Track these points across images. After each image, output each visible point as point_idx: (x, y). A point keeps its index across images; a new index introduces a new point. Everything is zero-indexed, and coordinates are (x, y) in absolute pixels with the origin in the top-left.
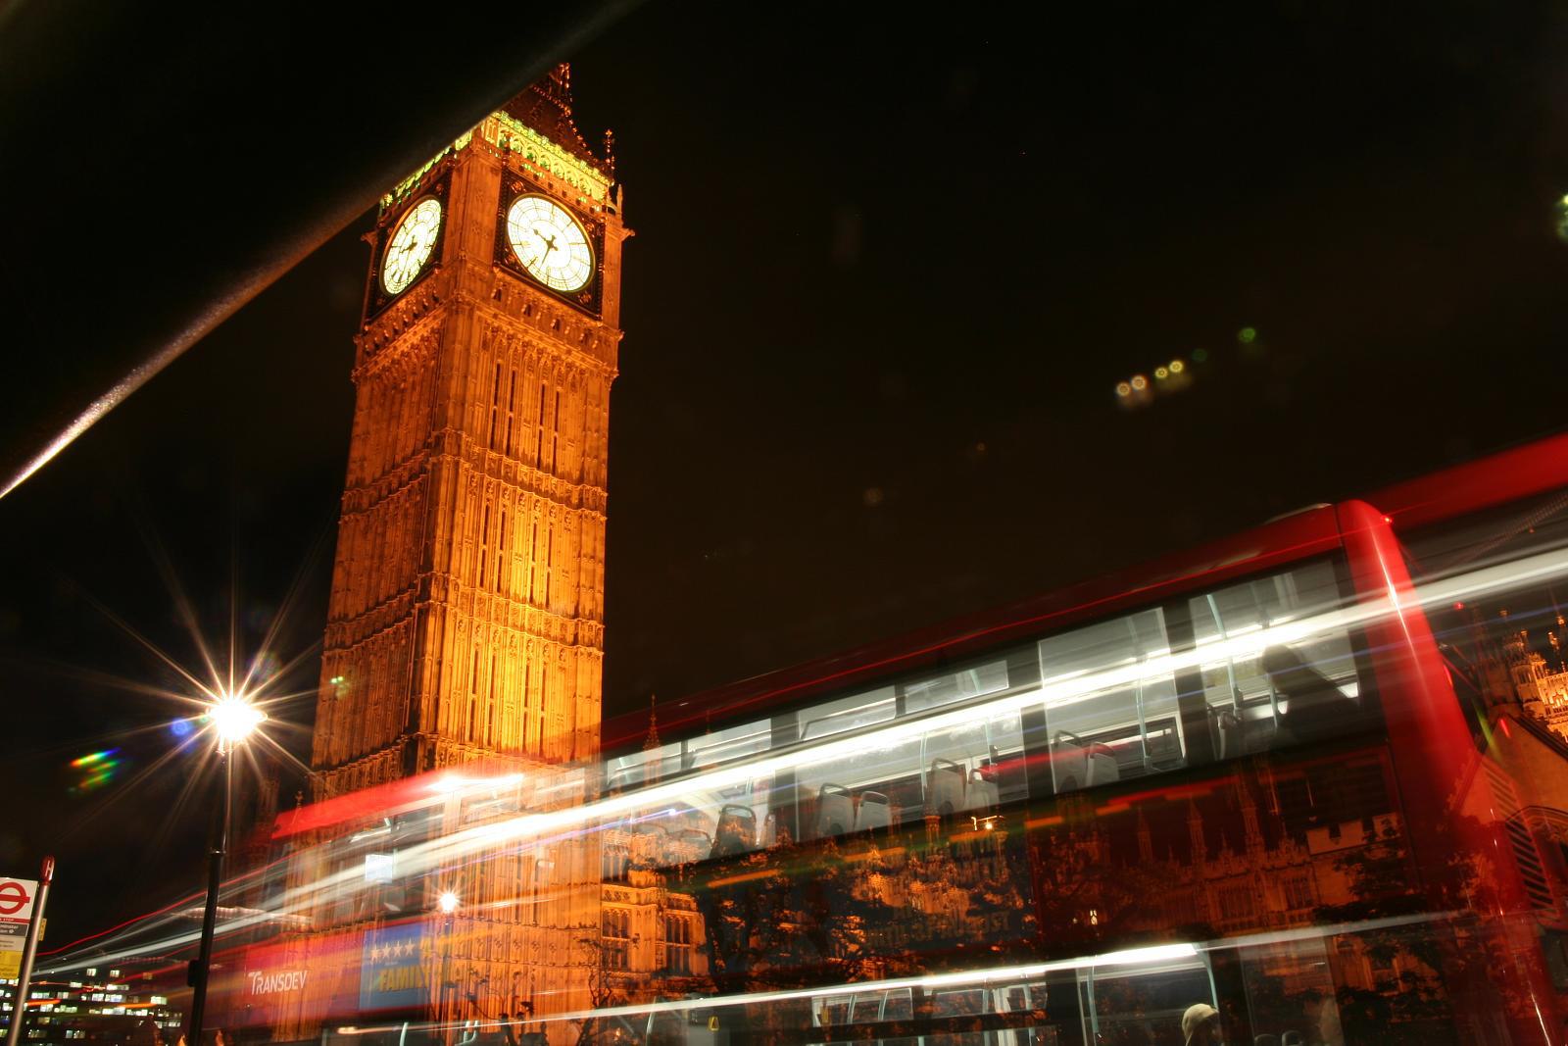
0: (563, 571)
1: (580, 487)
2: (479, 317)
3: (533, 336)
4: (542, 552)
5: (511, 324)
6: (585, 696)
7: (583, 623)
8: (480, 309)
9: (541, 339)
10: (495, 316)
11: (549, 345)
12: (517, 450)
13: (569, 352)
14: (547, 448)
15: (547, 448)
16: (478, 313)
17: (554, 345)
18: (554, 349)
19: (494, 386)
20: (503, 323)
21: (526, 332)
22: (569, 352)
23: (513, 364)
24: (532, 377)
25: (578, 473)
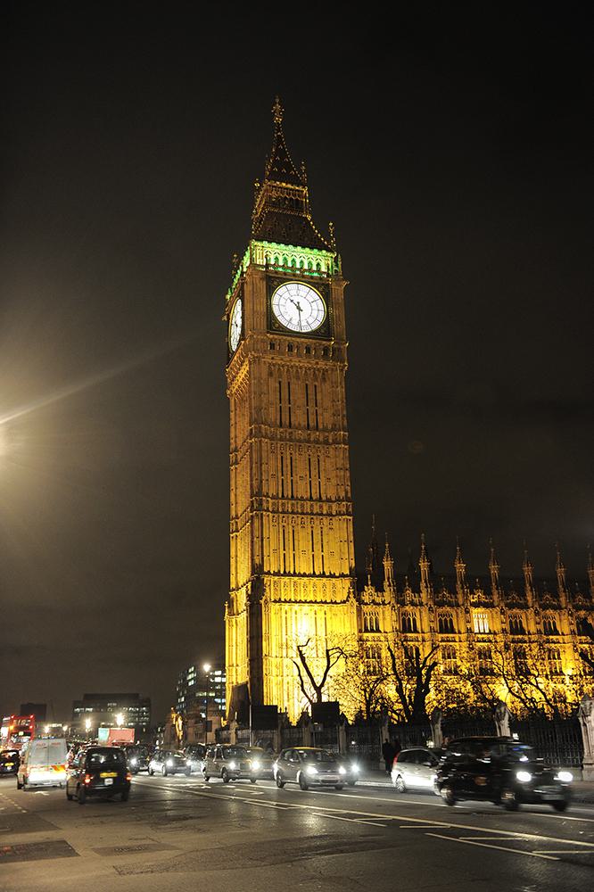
3: (295, 362)
10: (273, 358)
22: (317, 363)
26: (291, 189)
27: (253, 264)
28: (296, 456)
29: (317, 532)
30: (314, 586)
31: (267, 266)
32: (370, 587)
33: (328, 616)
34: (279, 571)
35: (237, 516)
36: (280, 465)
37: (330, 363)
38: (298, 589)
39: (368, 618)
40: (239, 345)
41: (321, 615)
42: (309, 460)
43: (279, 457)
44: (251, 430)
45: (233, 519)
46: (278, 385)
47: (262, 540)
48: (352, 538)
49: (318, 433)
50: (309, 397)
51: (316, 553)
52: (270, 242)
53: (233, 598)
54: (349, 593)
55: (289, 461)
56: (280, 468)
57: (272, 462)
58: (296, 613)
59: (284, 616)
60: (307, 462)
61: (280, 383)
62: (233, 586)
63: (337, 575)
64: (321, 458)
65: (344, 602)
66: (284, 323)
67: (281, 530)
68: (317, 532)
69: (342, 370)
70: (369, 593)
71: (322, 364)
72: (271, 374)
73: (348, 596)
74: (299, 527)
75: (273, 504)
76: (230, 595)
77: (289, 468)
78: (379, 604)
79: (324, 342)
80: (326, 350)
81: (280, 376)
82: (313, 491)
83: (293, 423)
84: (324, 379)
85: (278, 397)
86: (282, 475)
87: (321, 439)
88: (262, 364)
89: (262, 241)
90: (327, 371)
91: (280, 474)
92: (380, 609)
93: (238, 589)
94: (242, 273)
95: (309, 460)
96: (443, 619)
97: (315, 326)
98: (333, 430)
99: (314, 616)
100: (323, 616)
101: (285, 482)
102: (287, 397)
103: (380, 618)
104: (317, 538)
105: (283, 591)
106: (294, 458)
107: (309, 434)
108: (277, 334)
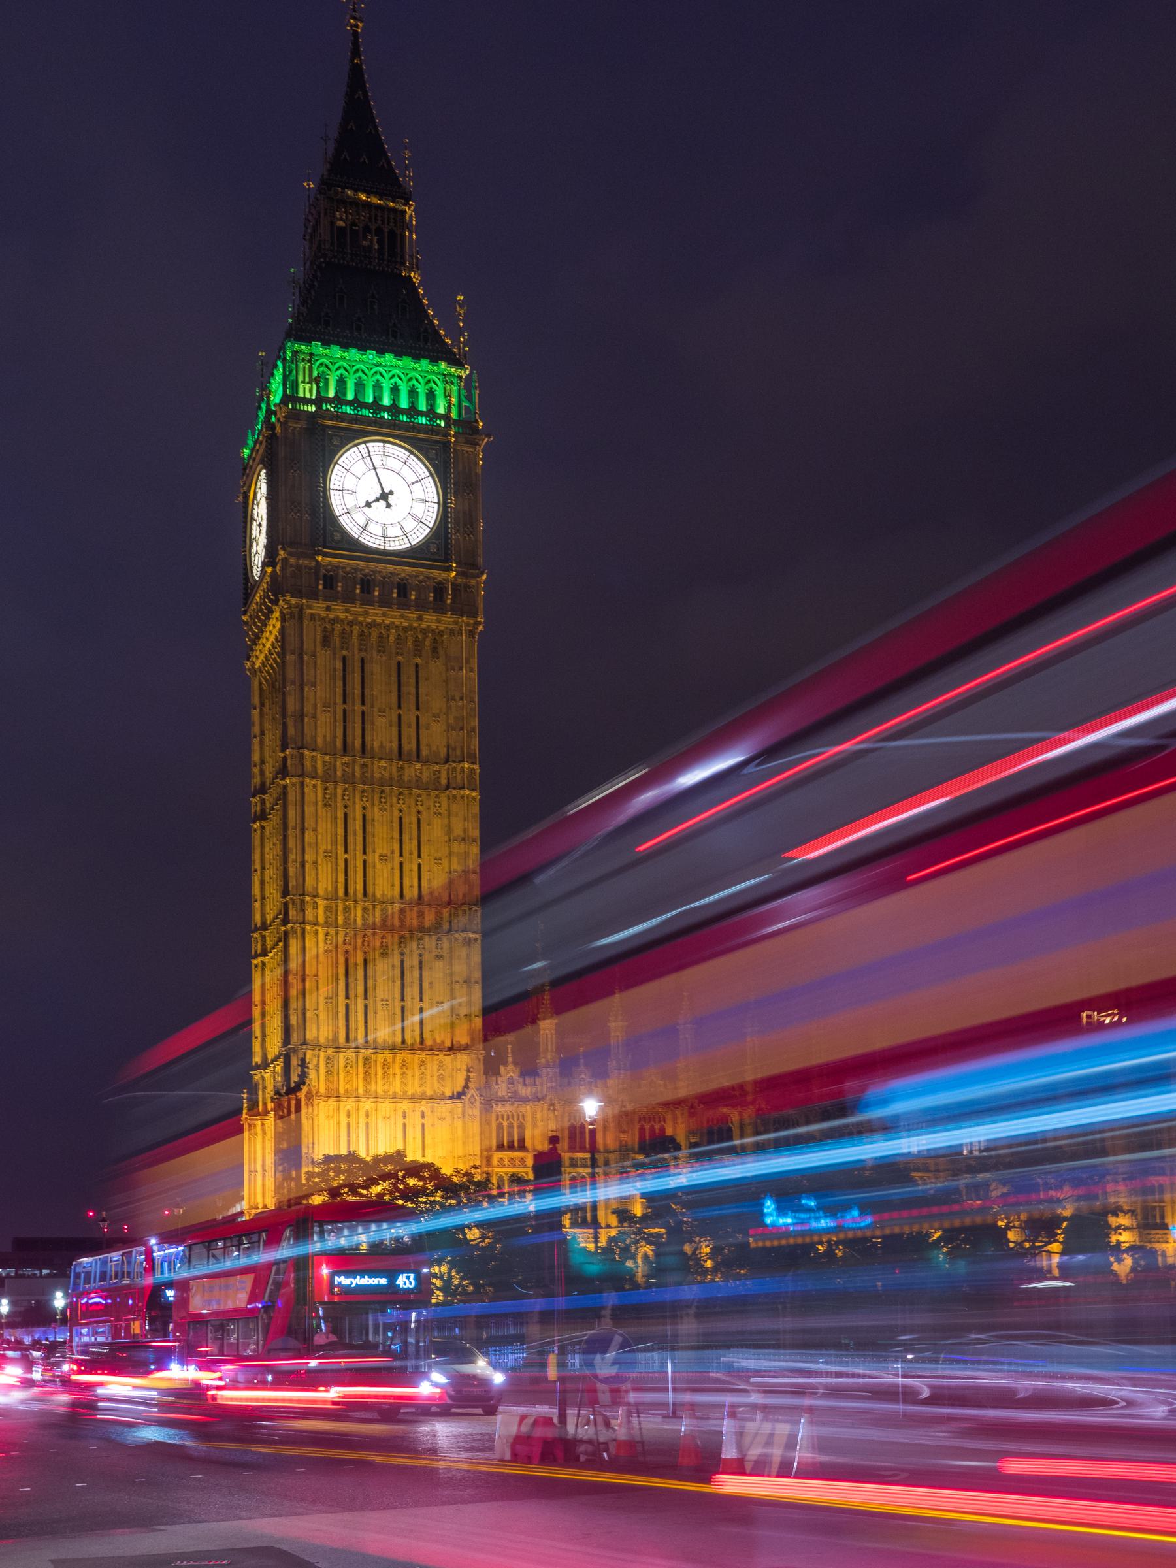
0: (435, 859)
1: (447, 766)
2: (312, 614)
3: (376, 614)
4: (410, 846)
5: (347, 611)
6: (461, 981)
7: (456, 909)
8: (310, 607)
9: (384, 615)
10: (328, 609)
11: (394, 618)
12: (372, 748)
13: (420, 618)
14: (409, 733)
15: (409, 733)
16: (308, 611)
17: (402, 617)
18: (403, 620)
19: (340, 683)
20: (340, 611)
21: (366, 613)
22: (420, 618)
23: (360, 650)
24: (384, 658)
25: (445, 749)
26: (378, 207)
27: (290, 398)
28: (375, 813)
29: (412, 961)
30: (404, 1065)
31: (320, 400)
32: (511, 1067)
33: (427, 1122)
34: (336, 1038)
35: (264, 923)
36: (341, 831)
37: (448, 619)
38: (372, 1071)
39: (505, 1124)
40: (263, 572)
41: (415, 1120)
42: (401, 819)
43: (340, 815)
44: (285, 759)
45: (256, 929)
46: (339, 665)
47: (304, 980)
48: (477, 975)
49: (418, 766)
50: (404, 689)
51: (408, 1004)
52: (326, 343)
53: (257, 1085)
54: (468, 1079)
55: (359, 823)
56: (340, 838)
57: (324, 826)
58: (367, 1116)
59: (343, 1120)
60: (396, 825)
61: (344, 659)
62: (257, 1059)
63: (448, 1044)
64: (424, 816)
65: (459, 1095)
66: (354, 531)
67: (342, 960)
68: (412, 961)
69: (471, 633)
70: (509, 1071)
71: (430, 620)
72: (326, 641)
73: (466, 1087)
74: (377, 953)
75: (327, 909)
76: (251, 1076)
77: (360, 838)
78: (525, 1100)
79: (435, 573)
80: (440, 590)
81: (345, 644)
82: (406, 882)
83: (368, 747)
84: (435, 650)
85: (339, 690)
86: (346, 852)
87: (424, 778)
88: (306, 622)
89: (307, 340)
90: (441, 633)
91: (341, 849)
92: (528, 1109)
93: (265, 1064)
94: (270, 413)
95: (401, 819)
96: (647, 1127)
97: (419, 535)
98: (447, 761)
99: (400, 1121)
100: (419, 1121)
101: (351, 867)
102: (358, 691)
103: (529, 1120)
104: (412, 976)
105: (342, 1075)
106: (369, 817)
107: (402, 768)
108: (336, 556)
